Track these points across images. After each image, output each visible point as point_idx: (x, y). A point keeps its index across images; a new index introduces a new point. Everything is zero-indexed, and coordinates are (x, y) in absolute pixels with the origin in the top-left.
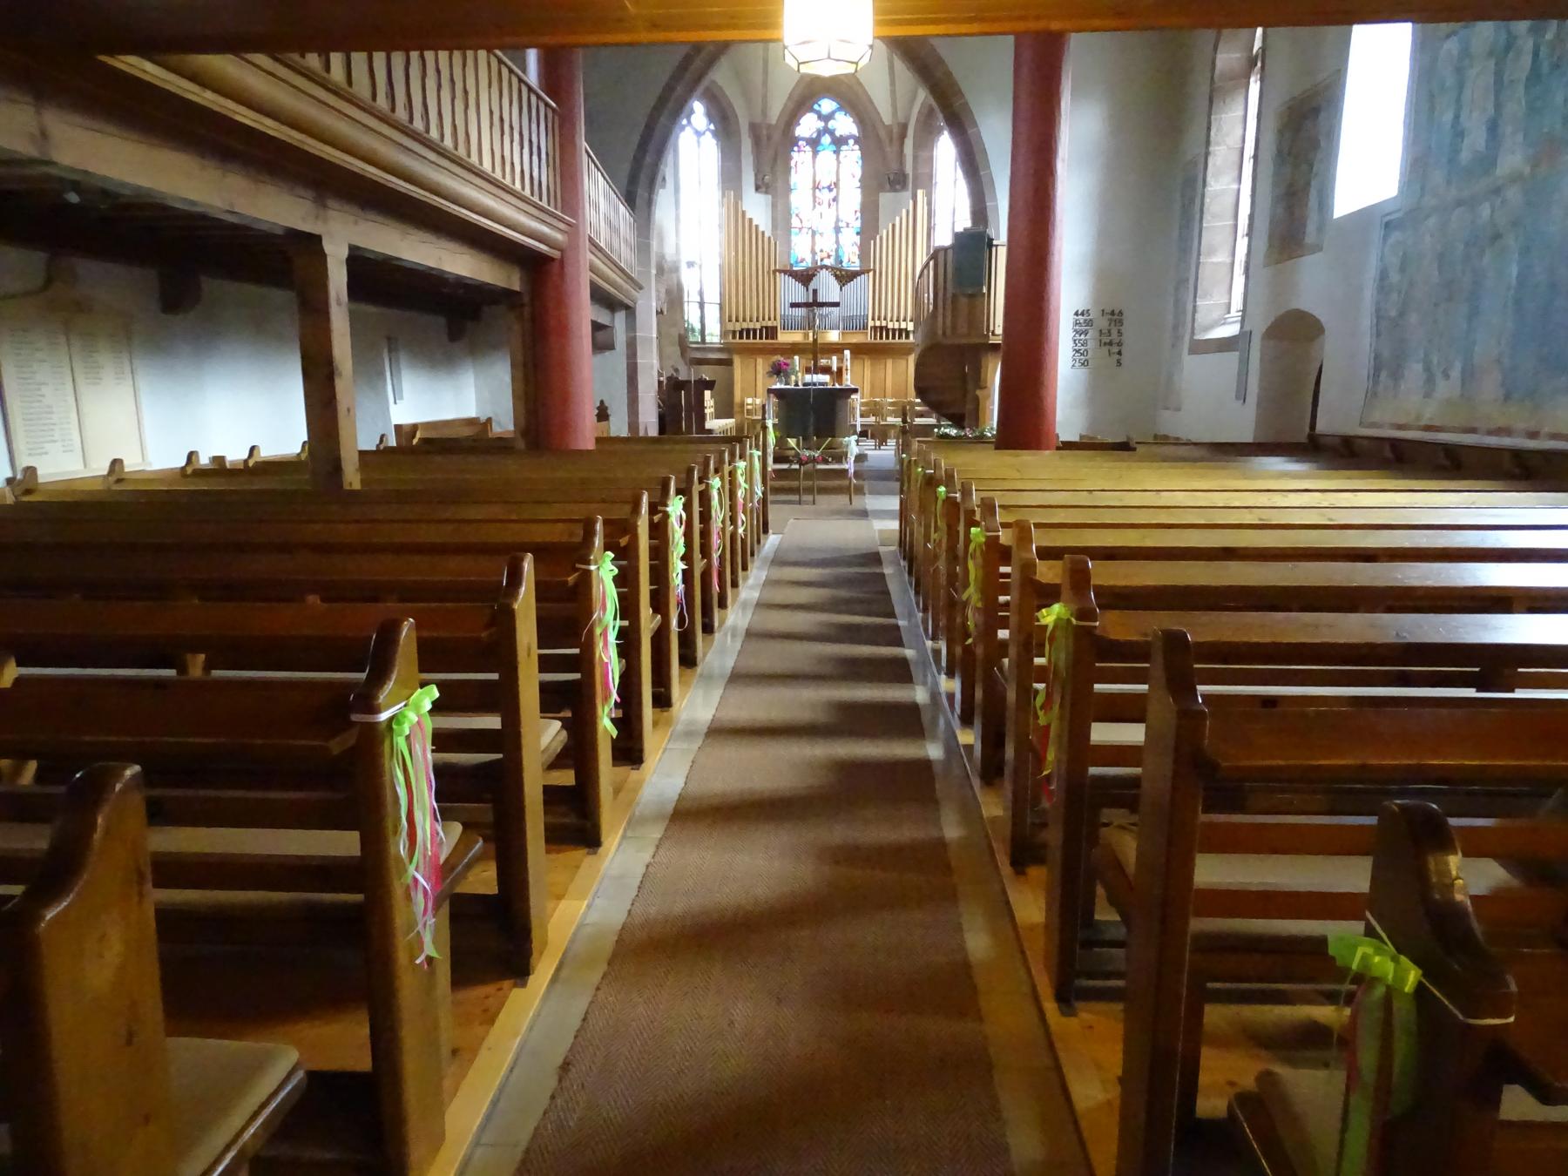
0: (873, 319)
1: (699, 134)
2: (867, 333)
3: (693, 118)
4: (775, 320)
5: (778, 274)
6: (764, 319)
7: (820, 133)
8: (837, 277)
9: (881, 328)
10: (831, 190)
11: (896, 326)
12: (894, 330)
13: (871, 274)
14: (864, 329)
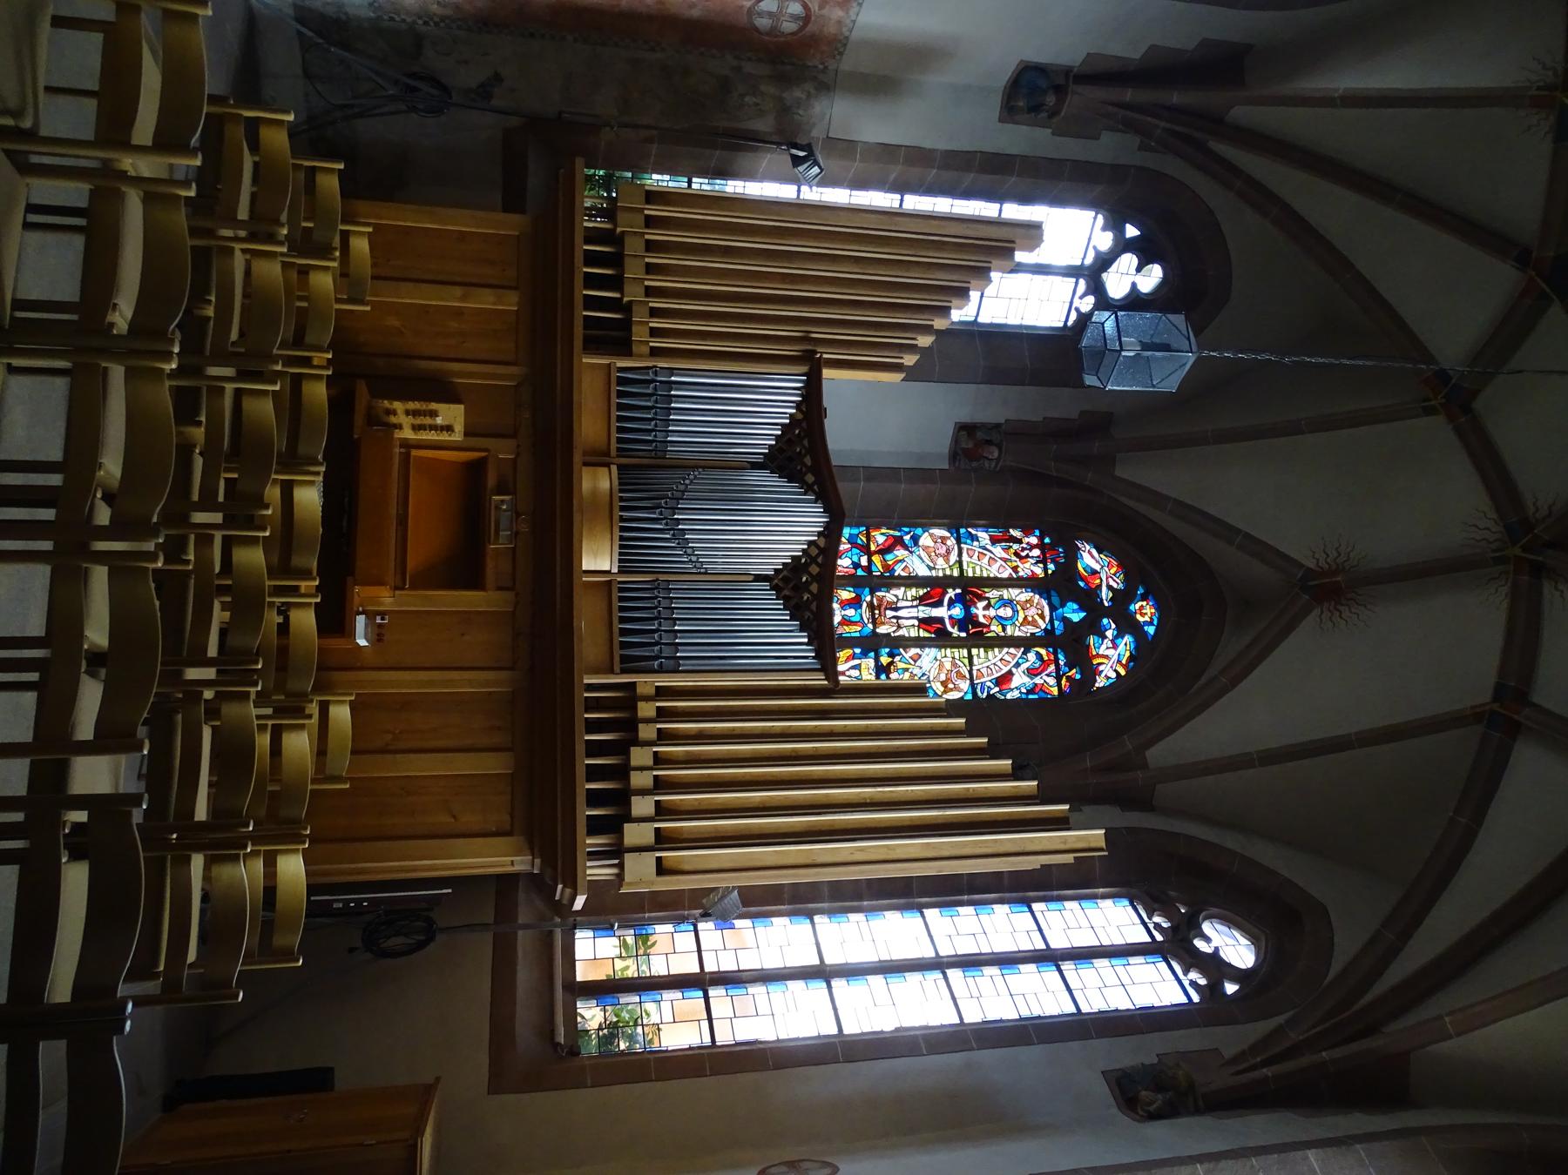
0: (662, 692)
1: (1093, 274)
2: (611, 671)
3: (1129, 260)
4: (655, 352)
5: (804, 369)
6: (654, 313)
7: (1088, 599)
8: (795, 567)
9: (630, 725)
10: (962, 624)
11: (639, 780)
14: (624, 659)
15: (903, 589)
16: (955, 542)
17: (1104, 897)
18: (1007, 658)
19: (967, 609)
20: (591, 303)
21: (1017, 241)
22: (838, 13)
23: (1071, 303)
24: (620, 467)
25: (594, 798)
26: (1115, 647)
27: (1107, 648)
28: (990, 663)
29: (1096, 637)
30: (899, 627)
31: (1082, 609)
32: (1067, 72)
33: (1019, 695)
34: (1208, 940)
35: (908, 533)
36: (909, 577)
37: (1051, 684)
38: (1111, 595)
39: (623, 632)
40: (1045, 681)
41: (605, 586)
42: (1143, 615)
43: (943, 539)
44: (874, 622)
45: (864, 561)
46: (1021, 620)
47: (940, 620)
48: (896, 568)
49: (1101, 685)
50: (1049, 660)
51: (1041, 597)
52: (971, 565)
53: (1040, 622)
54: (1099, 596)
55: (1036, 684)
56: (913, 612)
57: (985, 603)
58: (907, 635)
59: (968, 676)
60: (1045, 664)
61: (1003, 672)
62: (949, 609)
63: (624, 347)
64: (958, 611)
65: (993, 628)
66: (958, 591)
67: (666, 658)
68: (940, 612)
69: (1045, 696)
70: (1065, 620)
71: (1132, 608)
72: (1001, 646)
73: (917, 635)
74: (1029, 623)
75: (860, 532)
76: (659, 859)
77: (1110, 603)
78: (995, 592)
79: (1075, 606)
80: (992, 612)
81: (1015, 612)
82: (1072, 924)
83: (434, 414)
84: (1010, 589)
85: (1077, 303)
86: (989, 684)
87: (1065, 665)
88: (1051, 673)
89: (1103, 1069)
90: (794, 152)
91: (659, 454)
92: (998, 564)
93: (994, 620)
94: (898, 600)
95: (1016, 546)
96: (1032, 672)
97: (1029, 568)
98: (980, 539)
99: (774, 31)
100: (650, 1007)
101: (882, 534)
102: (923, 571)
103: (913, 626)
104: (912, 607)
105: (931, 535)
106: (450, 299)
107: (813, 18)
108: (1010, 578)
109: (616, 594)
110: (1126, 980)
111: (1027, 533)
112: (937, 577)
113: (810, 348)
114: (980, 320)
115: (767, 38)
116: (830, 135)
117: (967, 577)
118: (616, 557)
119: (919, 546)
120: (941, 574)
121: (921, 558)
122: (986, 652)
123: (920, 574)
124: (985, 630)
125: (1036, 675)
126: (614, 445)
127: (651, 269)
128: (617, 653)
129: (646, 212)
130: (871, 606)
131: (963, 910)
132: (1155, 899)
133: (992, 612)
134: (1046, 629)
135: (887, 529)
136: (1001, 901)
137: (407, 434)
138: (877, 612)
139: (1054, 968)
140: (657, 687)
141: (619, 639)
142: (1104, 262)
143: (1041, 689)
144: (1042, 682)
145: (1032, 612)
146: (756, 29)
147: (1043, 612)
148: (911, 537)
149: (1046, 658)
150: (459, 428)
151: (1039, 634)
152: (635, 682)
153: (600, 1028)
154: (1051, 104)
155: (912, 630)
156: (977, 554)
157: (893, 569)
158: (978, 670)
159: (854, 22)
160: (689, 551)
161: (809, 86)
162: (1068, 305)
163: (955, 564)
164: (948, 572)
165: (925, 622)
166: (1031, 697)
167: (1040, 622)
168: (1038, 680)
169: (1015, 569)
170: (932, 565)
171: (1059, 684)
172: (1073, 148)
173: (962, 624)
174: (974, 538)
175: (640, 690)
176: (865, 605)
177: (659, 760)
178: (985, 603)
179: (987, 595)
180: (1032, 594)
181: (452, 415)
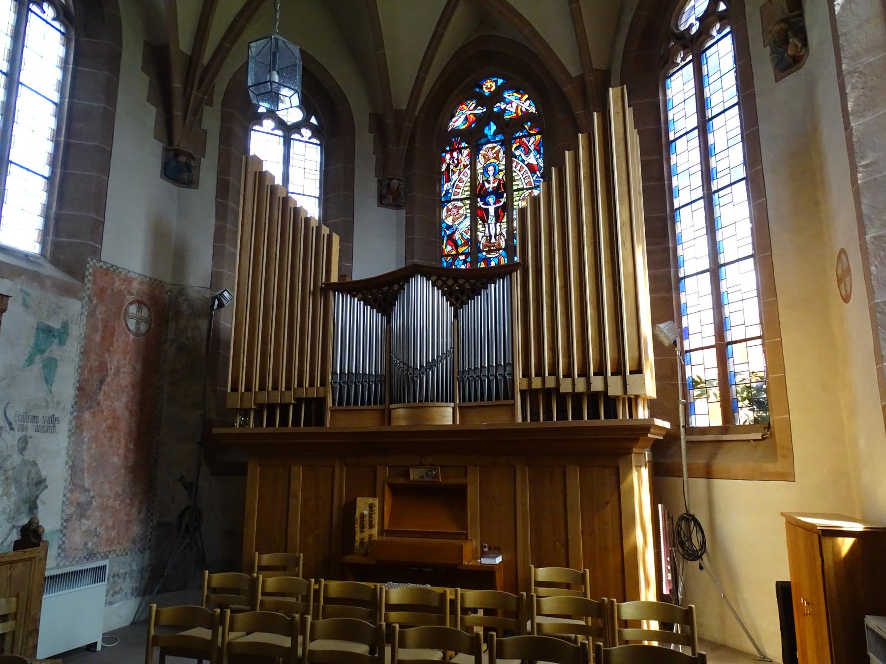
0: (526, 374)
1: (288, 131)
2: (513, 406)
4: (323, 383)
5: (331, 293)
6: (300, 385)
7: (482, 121)
9: (548, 393)
10: (499, 196)
11: (581, 386)
12: (577, 398)
13: (517, 276)
14: (506, 397)
15: (478, 233)
16: (450, 204)
17: (665, 95)
18: (518, 167)
19: (489, 194)
20: (296, 423)
21: (255, 171)
22: (135, 285)
23: (306, 142)
24: (391, 403)
25: (594, 415)
26: (511, 102)
27: (512, 107)
28: (522, 178)
29: (505, 115)
30: (501, 234)
31: (488, 125)
32: (166, 150)
33: (541, 159)
34: (691, 25)
35: (445, 232)
36: (471, 230)
37: (534, 140)
38: (480, 107)
39: (490, 398)
40: (532, 143)
41: (462, 410)
42: (491, 87)
43: (449, 210)
44: (498, 249)
45: (462, 257)
46: (495, 161)
47: (496, 209)
48: (466, 238)
49: (534, 109)
50: (519, 142)
51: (481, 149)
52: (463, 193)
53: (496, 149)
54: (480, 115)
55: (534, 149)
56: (492, 226)
57: (486, 183)
58: (506, 229)
59: (530, 191)
60: (522, 144)
61: (527, 169)
62: (490, 205)
63: (321, 402)
64: (491, 199)
65: (501, 177)
66: (479, 200)
67: (505, 371)
68: (492, 210)
69: (541, 143)
70: (495, 134)
71: (487, 94)
72: (512, 172)
73: (506, 223)
74: (498, 156)
75: (445, 261)
76: (631, 372)
77: (485, 107)
78: (479, 177)
79: (487, 128)
80: (491, 179)
81: (491, 164)
82: (682, 113)
83: (362, 516)
84: (477, 168)
85: (305, 139)
86: (534, 178)
87: (522, 132)
88: (527, 140)
89: (775, 82)
90: (215, 307)
91: (383, 378)
92: (463, 177)
93: (496, 177)
94: (485, 236)
95: (452, 167)
96: (527, 152)
97: (465, 159)
98: (448, 189)
99: (148, 321)
100: (738, 379)
101: (446, 247)
102: (467, 222)
103: (500, 226)
104: (489, 227)
105: (446, 218)
106: (297, 505)
107: (139, 299)
108: (470, 169)
109: (467, 404)
110: (718, 75)
111: (443, 160)
112: (471, 213)
113: (319, 290)
114: (318, 195)
115: (153, 325)
116: (209, 286)
117: (470, 195)
118: (444, 404)
119: (453, 225)
120: (469, 211)
121: (460, 223)
122: (515, 180)
123: (469, 223)
124: (502, 182)
125: (529, 149)
126: (378, 407)
127: (275, 388)
128: (502, 402)
129: (243, 391)
130: (488, 252)
131: (674, 184)
132: (667, 62)
133: (491, 179)
134: (501, 145)
135: (443, 244)
136: (669, 159)
137: (375, 531)
138: (492, 248)
139: (711, 122)
140: (523, 377)
141: (494, 401)
142: (281, 124)
143: (537, 146)
144: (533, 145)
145: (490, 154)
146: (148, 331)
147: (490, 148)
148: (447, 230)
149: (518, 144)
150: (370, 500)
151: (504, 149)
152: (521, 391)
153: (753, 410)
154: (185, 158)
155: (503, 227)
156: (457, 190)
157: (466, 240)
158: (526, 185)
159: (140, 274)
160: (440, 359)
161: (181, 300)
162: (308, 144)
163: (463, 203)
164: (468, 206)
165: (498, 219)
166: (542, 152)
167: (496, 149)
168: (532, 148)
169: (465, 166)
170: (464, 217)
171: (534, 135)
172: (212, 146)
173: (499, 196)
174: (447, 192)
175: (525, 387)
176: (488, 256)
177: (569, 374)
178: (486, 183)
179: (481, 182)
180: (480, 155)
181: (363, 505)
